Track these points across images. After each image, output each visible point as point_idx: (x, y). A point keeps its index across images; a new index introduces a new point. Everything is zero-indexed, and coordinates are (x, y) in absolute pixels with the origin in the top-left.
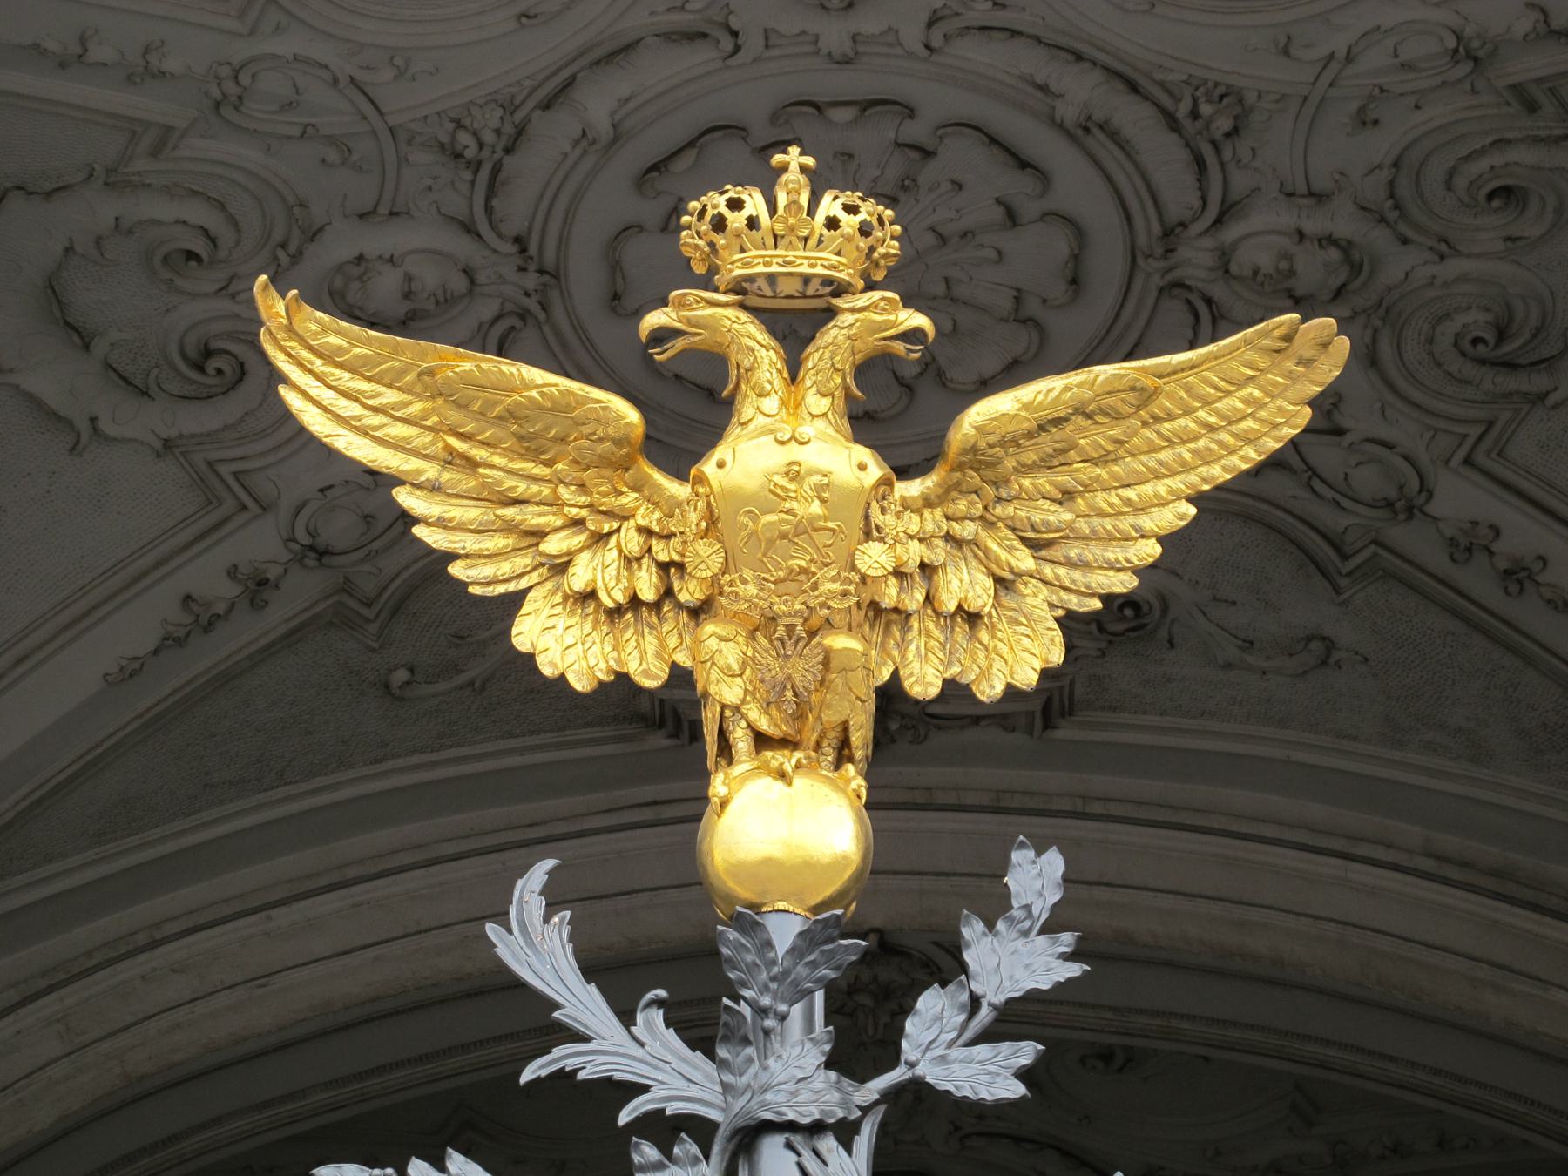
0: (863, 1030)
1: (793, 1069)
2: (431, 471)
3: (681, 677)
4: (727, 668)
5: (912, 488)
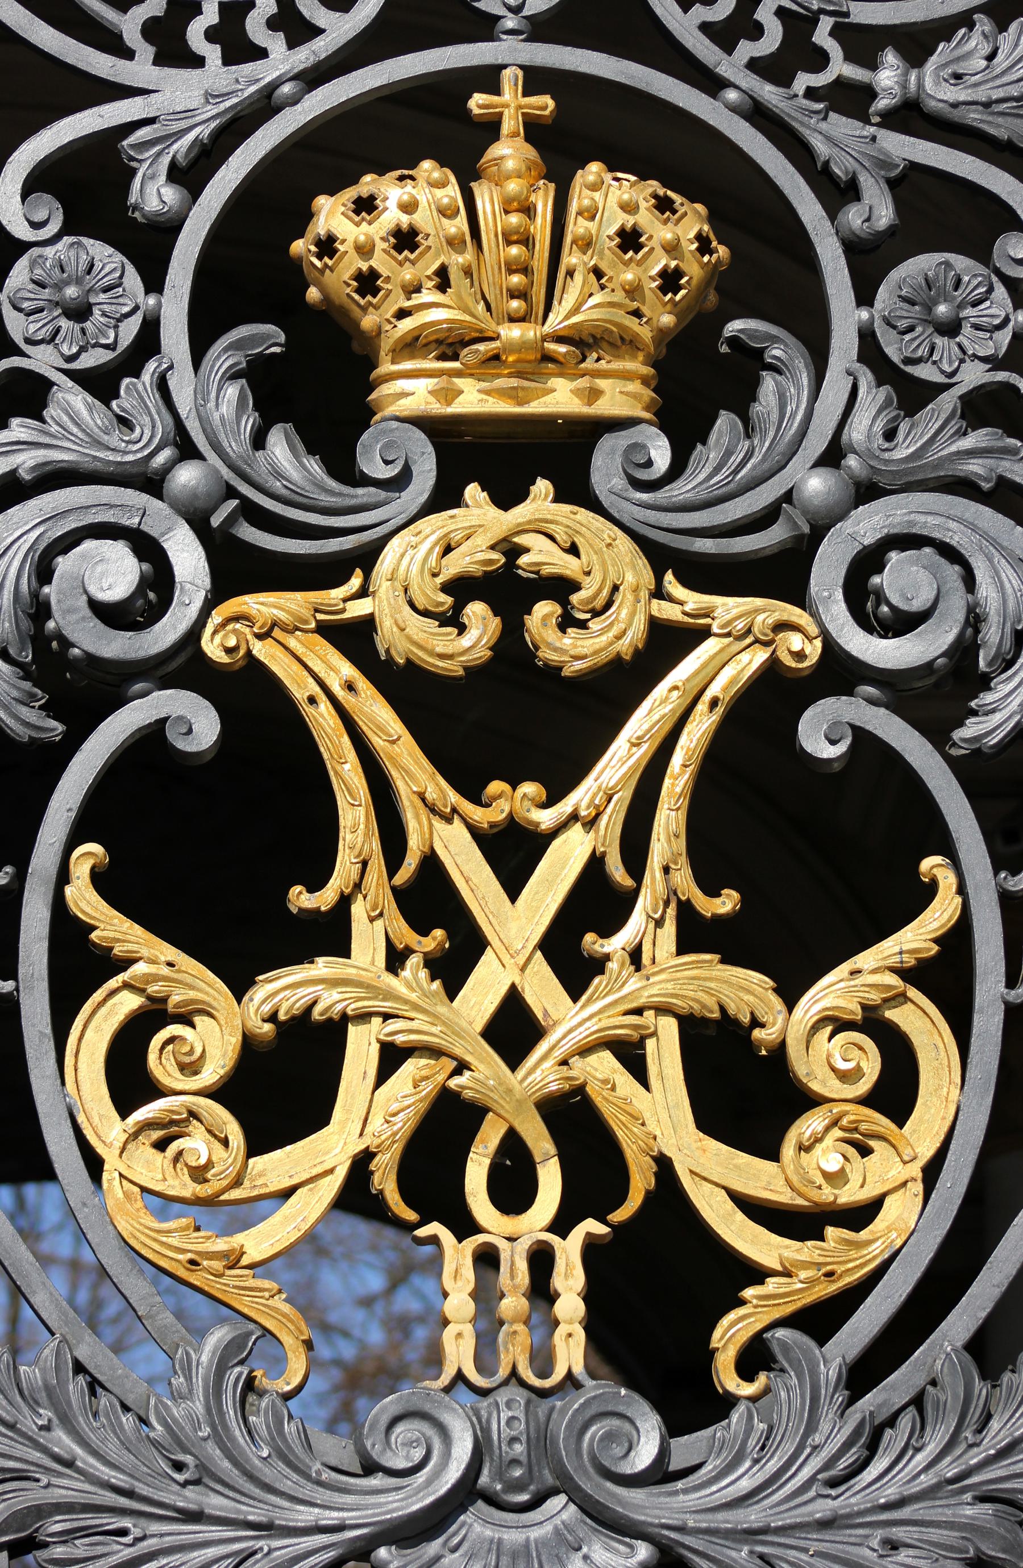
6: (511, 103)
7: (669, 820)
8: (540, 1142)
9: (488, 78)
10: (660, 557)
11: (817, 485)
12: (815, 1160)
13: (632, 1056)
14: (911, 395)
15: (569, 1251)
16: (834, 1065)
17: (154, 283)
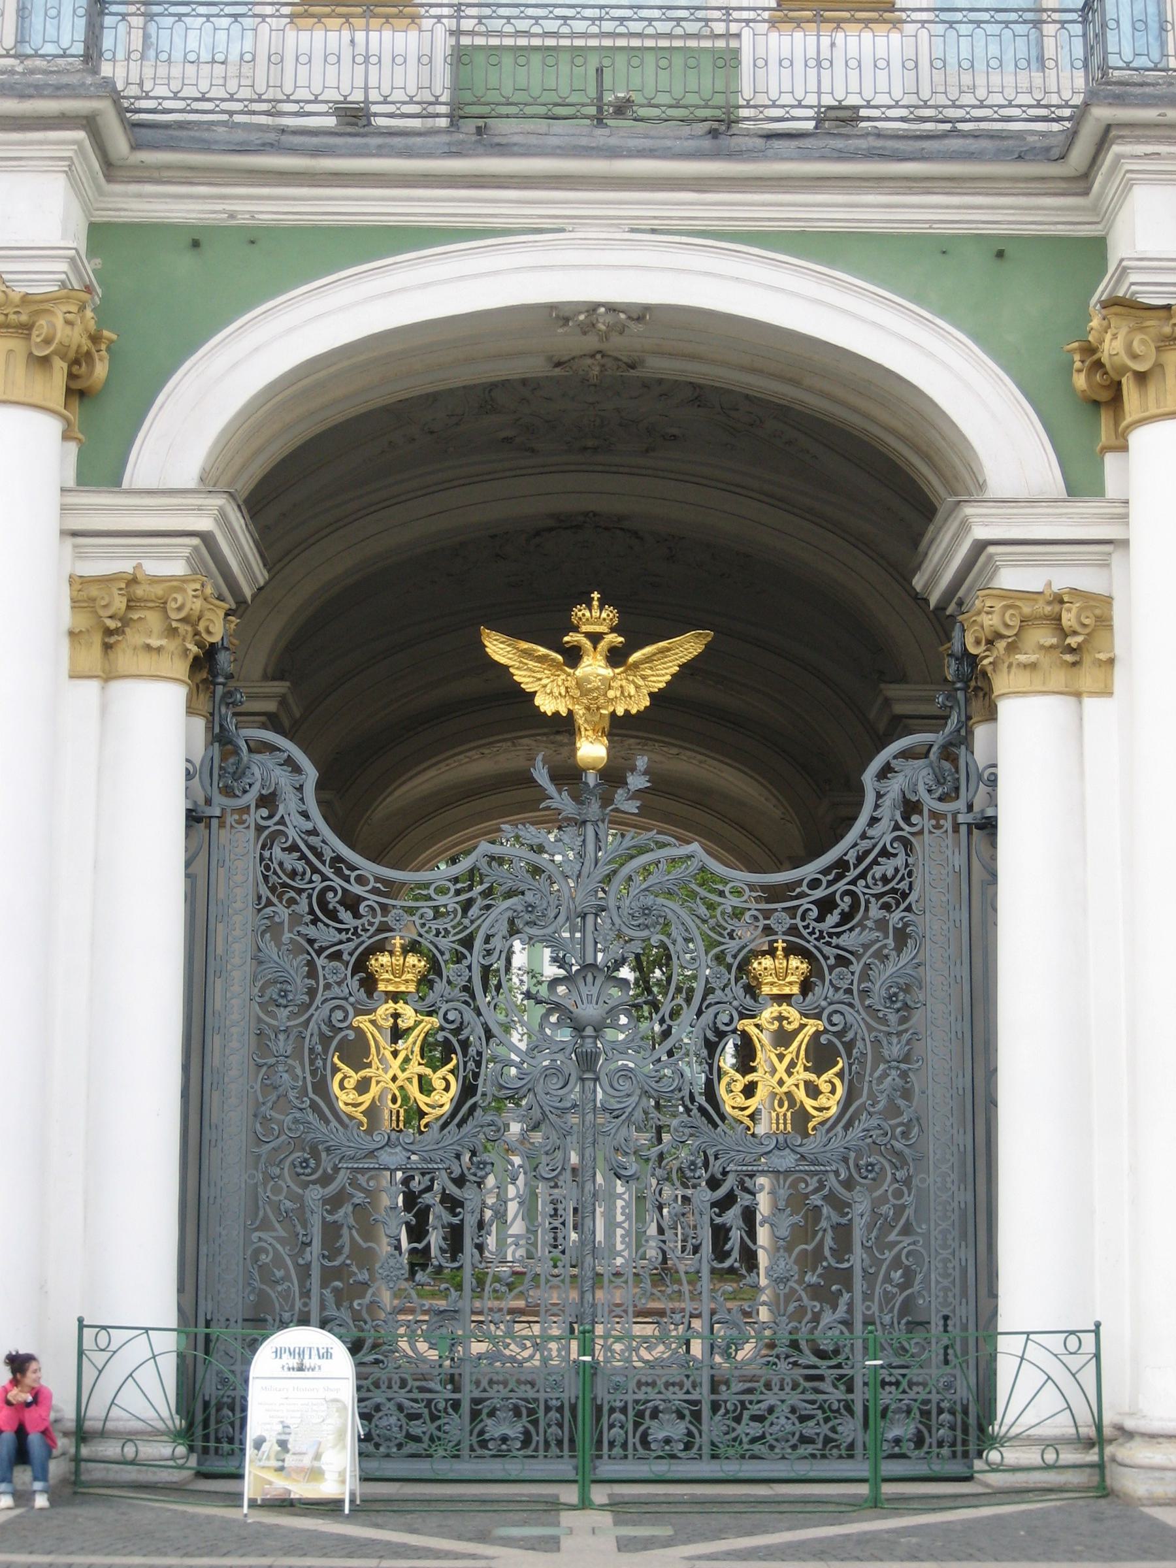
0: (607, 801)
1: (594, 809)
2: (517, 664)
3: (570, 712)
4: (579, 710)
5: (618, 671)
6: (780, 945)
7: (802, 1053)
8: (784, 1098)
9: (776, 941)
10: (802, 1014)
11: (824, 1003)
12: (822, 1101)
13: (797, 1086)
14: (837, 989)
15: (789, 1114)
16: (825, 1088)
17: (729, 973)
